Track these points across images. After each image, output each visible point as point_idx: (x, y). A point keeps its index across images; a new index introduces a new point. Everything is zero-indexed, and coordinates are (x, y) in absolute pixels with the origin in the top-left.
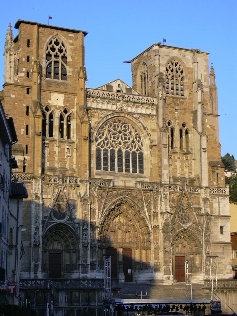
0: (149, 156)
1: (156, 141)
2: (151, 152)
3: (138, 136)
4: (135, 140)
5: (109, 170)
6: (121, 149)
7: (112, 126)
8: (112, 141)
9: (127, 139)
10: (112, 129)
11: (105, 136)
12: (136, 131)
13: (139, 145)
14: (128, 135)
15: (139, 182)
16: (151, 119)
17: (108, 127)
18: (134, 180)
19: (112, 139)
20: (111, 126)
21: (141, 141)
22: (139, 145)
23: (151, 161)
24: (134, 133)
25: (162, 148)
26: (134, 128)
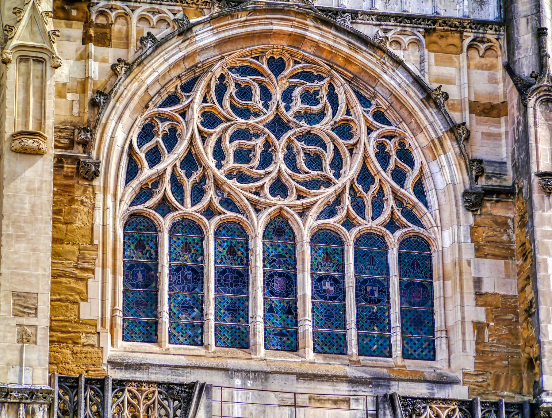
0: (468, 252)
1: (509, 166)
2: (473, 230)
3: (392, 146)
4: (375, 165)
5: (210, 337)
6: (286, 221)
7: (232, 89)
8: (229, 176)
9: (327, 164)
10: (226, 110)
11: (181, 149)
12: (379, 116)
13: (398, 200)
14: (327, 140)
15: (391, 399)
16: (470, 47)
17: (205, 100)
18: (366, 391)
19: (230, 163)
20: (221, 90)
21: (416, 172)
22: (398, 200)
23: (478, 282)
24: (370, 130)
25: (536, 197)
26: (365, 102)
